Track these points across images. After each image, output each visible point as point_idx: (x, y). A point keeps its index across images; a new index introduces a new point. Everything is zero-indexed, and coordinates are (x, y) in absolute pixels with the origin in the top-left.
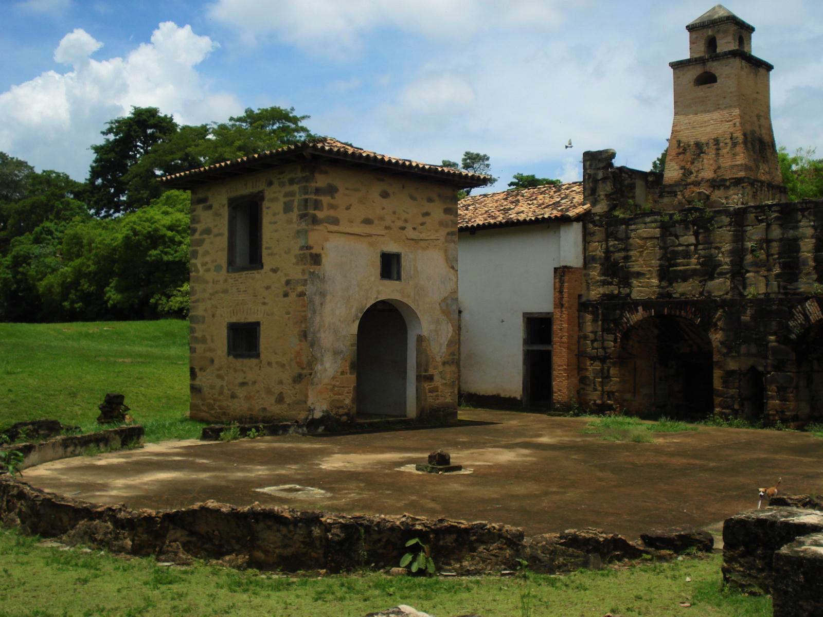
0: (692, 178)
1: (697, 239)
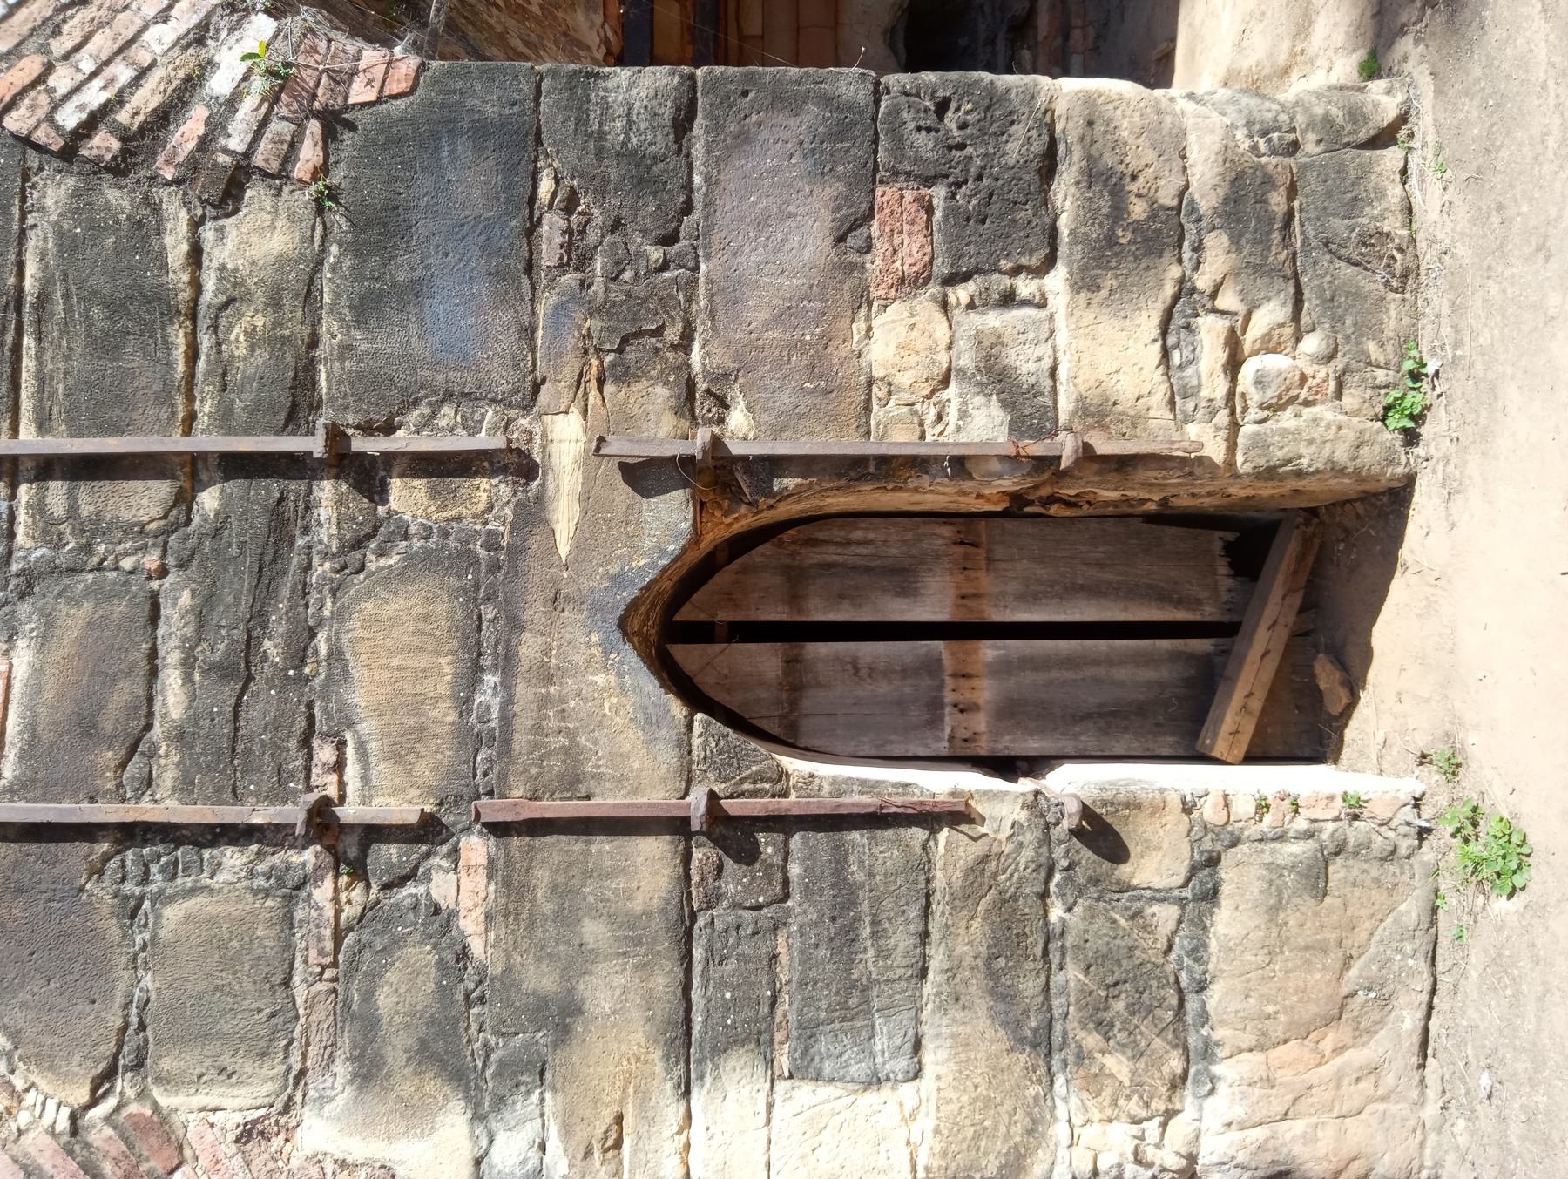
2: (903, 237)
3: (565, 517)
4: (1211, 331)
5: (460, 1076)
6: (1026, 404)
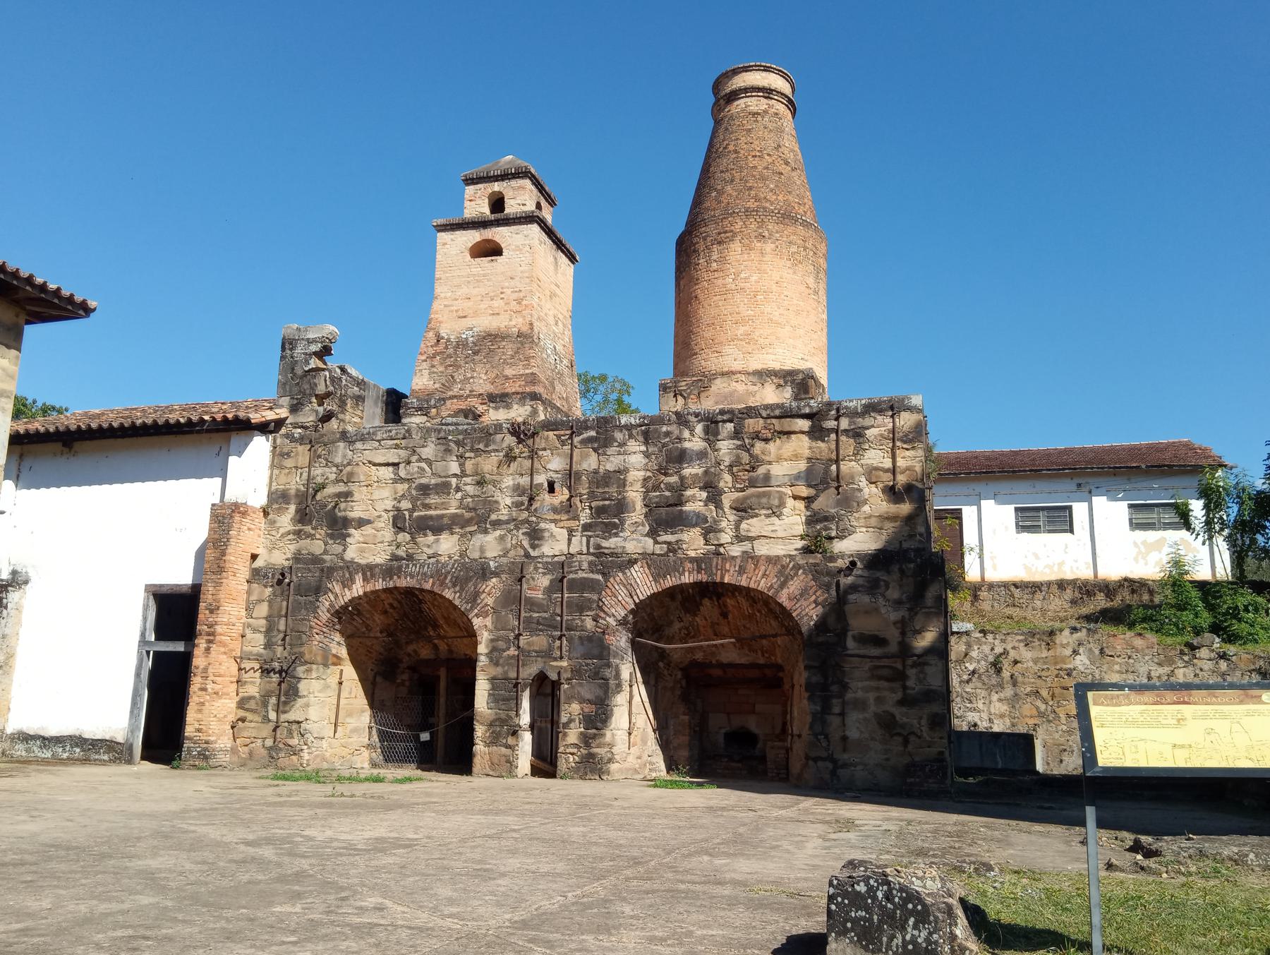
0: (456, 390)
1: (462, 465)
2: (589, 708)
3: (554, 664)
4: (575, 750)
5: (491, 652)
6: (566, 725)
